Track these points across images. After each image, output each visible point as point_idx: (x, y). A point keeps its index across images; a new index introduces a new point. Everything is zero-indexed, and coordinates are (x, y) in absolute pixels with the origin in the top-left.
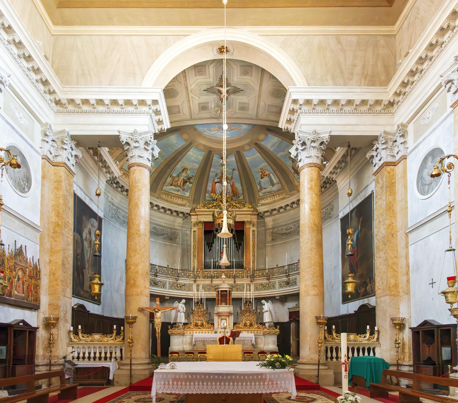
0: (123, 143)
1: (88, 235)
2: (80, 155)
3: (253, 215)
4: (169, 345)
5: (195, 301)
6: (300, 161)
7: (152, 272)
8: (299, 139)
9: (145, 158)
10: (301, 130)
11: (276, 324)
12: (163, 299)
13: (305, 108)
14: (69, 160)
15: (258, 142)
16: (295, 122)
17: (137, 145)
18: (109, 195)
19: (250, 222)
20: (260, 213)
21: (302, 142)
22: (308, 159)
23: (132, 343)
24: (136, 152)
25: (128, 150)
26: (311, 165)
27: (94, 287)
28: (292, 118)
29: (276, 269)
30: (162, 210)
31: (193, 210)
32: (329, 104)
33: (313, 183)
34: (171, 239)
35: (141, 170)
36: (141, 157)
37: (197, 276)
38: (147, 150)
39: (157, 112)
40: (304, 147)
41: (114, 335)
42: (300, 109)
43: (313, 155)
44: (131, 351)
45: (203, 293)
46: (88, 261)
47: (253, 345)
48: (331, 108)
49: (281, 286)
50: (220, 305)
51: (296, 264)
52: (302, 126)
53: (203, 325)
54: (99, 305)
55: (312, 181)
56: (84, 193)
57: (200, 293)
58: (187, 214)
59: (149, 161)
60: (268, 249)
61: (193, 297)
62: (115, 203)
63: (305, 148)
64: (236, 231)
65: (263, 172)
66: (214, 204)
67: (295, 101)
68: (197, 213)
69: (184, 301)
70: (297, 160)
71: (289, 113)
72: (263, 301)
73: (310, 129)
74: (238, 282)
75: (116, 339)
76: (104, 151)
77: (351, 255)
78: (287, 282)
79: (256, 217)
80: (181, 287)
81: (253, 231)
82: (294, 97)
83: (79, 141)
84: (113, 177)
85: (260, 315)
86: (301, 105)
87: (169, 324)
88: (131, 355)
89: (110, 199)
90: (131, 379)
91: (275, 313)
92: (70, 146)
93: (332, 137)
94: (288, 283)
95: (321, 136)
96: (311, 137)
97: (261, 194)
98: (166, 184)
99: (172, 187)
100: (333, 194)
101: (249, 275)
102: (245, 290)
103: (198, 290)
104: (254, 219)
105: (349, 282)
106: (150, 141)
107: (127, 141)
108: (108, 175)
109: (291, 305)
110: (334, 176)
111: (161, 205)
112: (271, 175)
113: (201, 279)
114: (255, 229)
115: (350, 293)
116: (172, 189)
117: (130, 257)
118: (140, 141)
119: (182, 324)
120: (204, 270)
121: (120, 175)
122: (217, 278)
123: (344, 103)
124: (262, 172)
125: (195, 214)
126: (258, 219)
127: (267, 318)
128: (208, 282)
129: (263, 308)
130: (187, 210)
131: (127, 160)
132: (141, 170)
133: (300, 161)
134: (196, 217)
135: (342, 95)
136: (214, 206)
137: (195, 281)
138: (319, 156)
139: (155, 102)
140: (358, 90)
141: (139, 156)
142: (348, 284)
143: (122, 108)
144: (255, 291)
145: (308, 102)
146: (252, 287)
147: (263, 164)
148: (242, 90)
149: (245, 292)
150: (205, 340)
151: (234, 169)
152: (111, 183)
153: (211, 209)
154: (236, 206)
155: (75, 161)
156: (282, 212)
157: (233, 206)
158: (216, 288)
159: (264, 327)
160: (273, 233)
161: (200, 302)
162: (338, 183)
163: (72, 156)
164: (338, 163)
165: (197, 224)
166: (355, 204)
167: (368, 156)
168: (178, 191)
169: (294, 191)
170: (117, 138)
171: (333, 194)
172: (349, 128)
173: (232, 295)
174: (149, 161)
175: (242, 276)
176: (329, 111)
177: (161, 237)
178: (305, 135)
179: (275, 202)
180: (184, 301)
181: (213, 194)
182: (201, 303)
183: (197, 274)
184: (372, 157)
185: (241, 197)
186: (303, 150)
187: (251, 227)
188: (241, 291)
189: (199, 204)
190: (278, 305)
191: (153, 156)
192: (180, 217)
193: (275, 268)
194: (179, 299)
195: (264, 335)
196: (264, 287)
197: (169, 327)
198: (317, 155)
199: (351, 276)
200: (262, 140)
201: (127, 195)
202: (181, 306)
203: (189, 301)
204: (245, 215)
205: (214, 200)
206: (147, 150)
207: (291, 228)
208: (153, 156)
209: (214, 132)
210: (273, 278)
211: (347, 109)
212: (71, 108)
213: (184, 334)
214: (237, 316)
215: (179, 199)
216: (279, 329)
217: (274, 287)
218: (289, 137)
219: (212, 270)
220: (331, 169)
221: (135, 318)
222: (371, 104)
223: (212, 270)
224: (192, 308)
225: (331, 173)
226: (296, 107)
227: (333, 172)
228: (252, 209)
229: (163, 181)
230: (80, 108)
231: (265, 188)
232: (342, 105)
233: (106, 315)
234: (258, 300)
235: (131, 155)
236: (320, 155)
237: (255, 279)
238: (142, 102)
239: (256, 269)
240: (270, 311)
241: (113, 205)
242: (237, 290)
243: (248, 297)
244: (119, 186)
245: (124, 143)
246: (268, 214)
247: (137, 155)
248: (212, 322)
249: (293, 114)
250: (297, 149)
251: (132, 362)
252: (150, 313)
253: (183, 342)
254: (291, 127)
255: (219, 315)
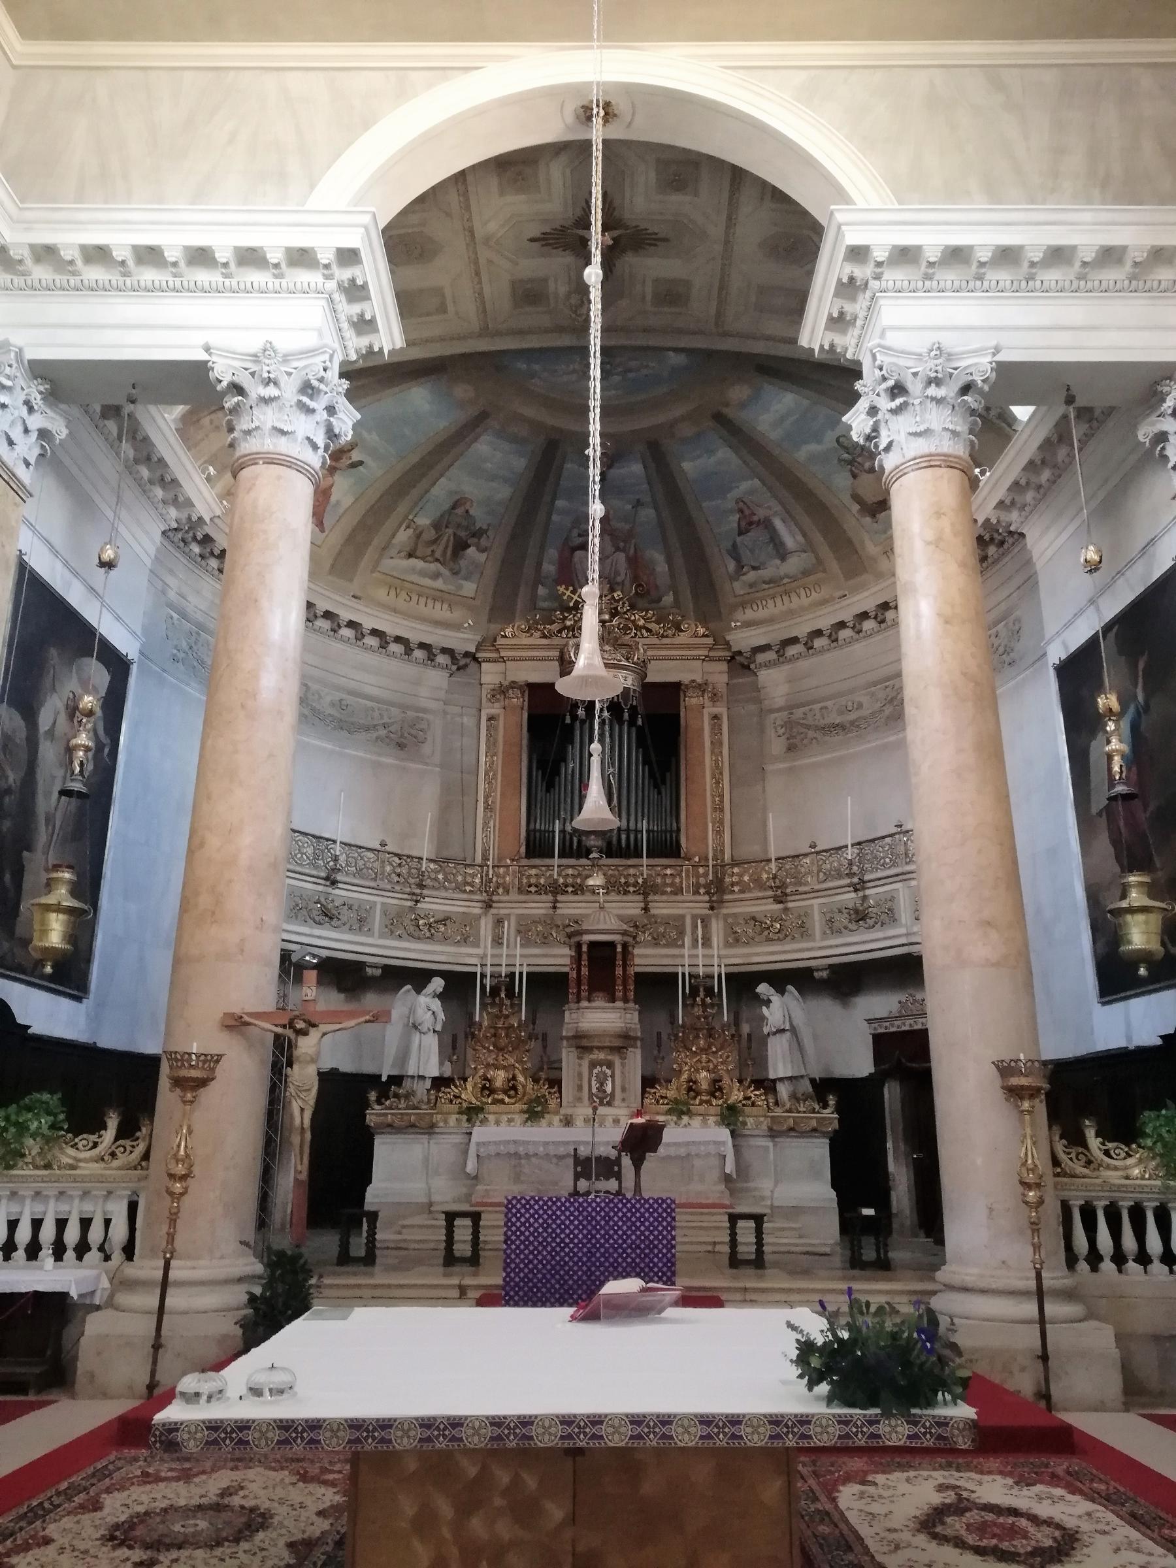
0: (219, 388)
1: (62, 719)
2: (60, 430)
3: (712, 659)
4: (366, 1177)
5: (483, 986)
6: (888, 449)
7: (316, 867)
8: (877, 373)
9: (300, 435)
10: (883, 342)
11: (824, 1087)
12: (344, 975)
13: (893, 276)
14: (11, 443)
15: (725, 411)
16: (859, 323)
17: (271, 391)
18: (171, 581)
19: (702, 688)
20: (740, 653)
21: (891, 383)
22: (921, 440)
23: (183, 1178)
24: (266, 417)
25: (235, 410)
26: (930, 462)
27: (44, 923)
28: (849, 308)
29: (807, 860)
30: (372, 641)
31: (489, 641)
32: (983, 260)
33: (946, 523)
34: (401, 746)
35: (279, 478)
36: (283, 433)
37: (498, 886)
38: (311, 411)
39: (355, 291)
40: (899, 401)
41: (109, 1135)
42: (878, 277)
43: (936, 426)
44: (173, 1219)
45: (518, 951)
46: (49, 819)
47: (727, 1178)
48: (992, 275)
49: (831, 927)
50: (584, 1004)
51: (888, 840)
52: (888, 334)
53: (514, 1088)
54: (78, 999)
55: (939, 514)
56: (66, 564)
57: (505, 951)
58: (467, 654)
59: (315, 447)
60: (774, 785)
61: (479, 970)
62: (190, 609)
63: (906, 404)
64: (648, 718)
65: (747, 512)
66: (568, 623)
67: (858, 254)
68: (502, 654)
69: (438, 984)
70: (876, 446)
71: (837, 294)
72: (763, 989)
73: (920, 343)
74: (662, 908)
75: (113, 1155)
76: (163, 422)
77: (1126, 797)
78: (857, 911)
79: (724, 666)
80: (436, 927)
81: (715, 717)
82: (853, 238)
83: (58, 382)
84: (189, 518)
85: (752, 1051)
86: (879, 264)
87: (373, 1080)
88: (171, 1238)
89: (172, 595)
90: (155, 1362)
91: (816, 1037)
92: (23, 397)
93: (1005, 370)
94: (860, 916)
95: (963, 364)
96: (926, 368)
97: (739, 587)
98: (393, 552)
99: (413, 561)
100: (1017, 581)
101: (702, 881)
102: (687, 940)
103: (497, 941)
104: (718, 674)
105: (1132, 910)
106: (321, 380)
107: (235, 379)
108: (173, 513)
109: (880, 1005)
110: (1014, 516)
111: (368, 624)
112: (778, 523)
113: (514, 896)
114: (721, 710)
115: (1144, 957)
116: (413, 570)
117: (209, 798)
118: (283, 380)
119: (428, 1084)
120: (525, 862)
121: (218, 513)
122: (575, 893)
123: (1037, 256)
124: (741, 511)
125: (494, 655)
126: (731, 673)
127: (780, 1064)
128: (538, 907)
129: (763, 1018)
130: (464, 641)
131: (232, 445)
132: (279, 478)
133: (888, 449)
134: (499, 667)
135: (1033, 232)
136: (565, 628)
137: (488, 905)
138: (958, 429)
139: (349, 256)
140: (1087, 217)
141: (275, 428)
142: (1129, 917)
143: (226, 276)
144: (727, 945)
145: (905, 255)
146: (717, 929)
147: (745, 486)
148: (666, 240)
149: (686, 952)
150: (521, 1150)
151: (638, 504)
152: (183, 540)
153: (556, 641)
154: (649, 630)
155: (37, 451)
156: (822, 651)
157: (638, 628)
158: (573, 935)
159: (771, 1101)
160: (789, 724)
161: (505, 987)
162: (1029, 540)
163: (26, 431)
164: (1040, 448)
165: (501, 691)
166: (1112, 607)
167: (1145, 433)
168: (436, 576)
169: (865, 577)
170: (200, 369)
171: (1017, 581)
172: (1064, 338)
173: (637, 961)
174: (315, 447)
175: (672, 885)
176: (986, 284)
177: (362, 736)
178: (902, 362)
179: (791, 614)
180: (438, 984)
181: (561, 589)
182: (510, 993)
183: (498, 876)
184: (1162, 437)
185: (668, 599)
186: (895, 412)
187: (707, 703)
188: (673, 944)
189: (510, 620)
190: (825, 1006)
191: (331, 434)
192: (439, 666)
193: (805, 855)
194: (418, 978)
195: (773, 1134)
196: (762, 929)
197: (373, 1096)
198: (951, 427)
199: (1141, 884)
200: (743, 405)
201: (221, 571)
202: (427, 1006)
203: (458, 985)
204: (678, 661)
205: (569, 610)
206: (311, 411)
207: (860, 706)
208: (331, 434)
209: (565, 378)
210: (797, 893)
211: (1051, 276)
212: (41, 273)
213: (433, 1126)
214: (655, 1047)
215: (438, 605)
216: (838, 1110)
217: (803, 930)
218: (836, 379)
219: (556, 861)
220: (1001, 493)
221: (212, 1061)
222: (1138, 260)
223: (556, 861)
224: (471, 1015)
225: (1001, 505)
226: (862, 272)
227: (1008, 502)
228: (710, 640)
229: (378, 541)
230: (74, 273)
231: (754, 568)
232: (1033, 264)
233: (109, 1040)
234: (743, 984)
235: (245, 427)
236: (962, 427)
237: (726, 897)
238: (301, 257)
239: (727, 857)
240: (793, 1030)
241: (183, 615)
242: (656, 942)
243: (701, 971)
244: (212, 554)
245: (224, 384)
246: (771, 655)
247: (269, 425)
248: (553, 1075)
249: (853, 299)
250: (873, 411)
251: (173, 1275)
252: (277, 1037)
253: (426, 1160)
254: (848, 344)
255: (582, 1043)
